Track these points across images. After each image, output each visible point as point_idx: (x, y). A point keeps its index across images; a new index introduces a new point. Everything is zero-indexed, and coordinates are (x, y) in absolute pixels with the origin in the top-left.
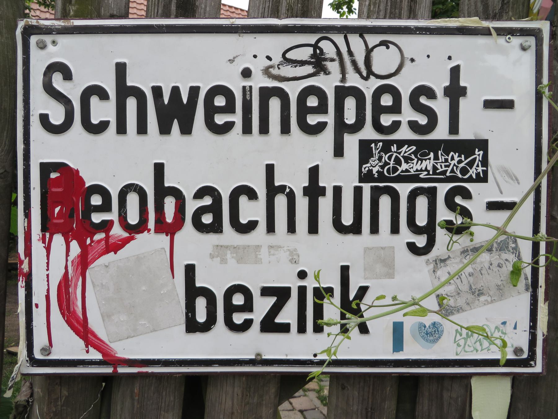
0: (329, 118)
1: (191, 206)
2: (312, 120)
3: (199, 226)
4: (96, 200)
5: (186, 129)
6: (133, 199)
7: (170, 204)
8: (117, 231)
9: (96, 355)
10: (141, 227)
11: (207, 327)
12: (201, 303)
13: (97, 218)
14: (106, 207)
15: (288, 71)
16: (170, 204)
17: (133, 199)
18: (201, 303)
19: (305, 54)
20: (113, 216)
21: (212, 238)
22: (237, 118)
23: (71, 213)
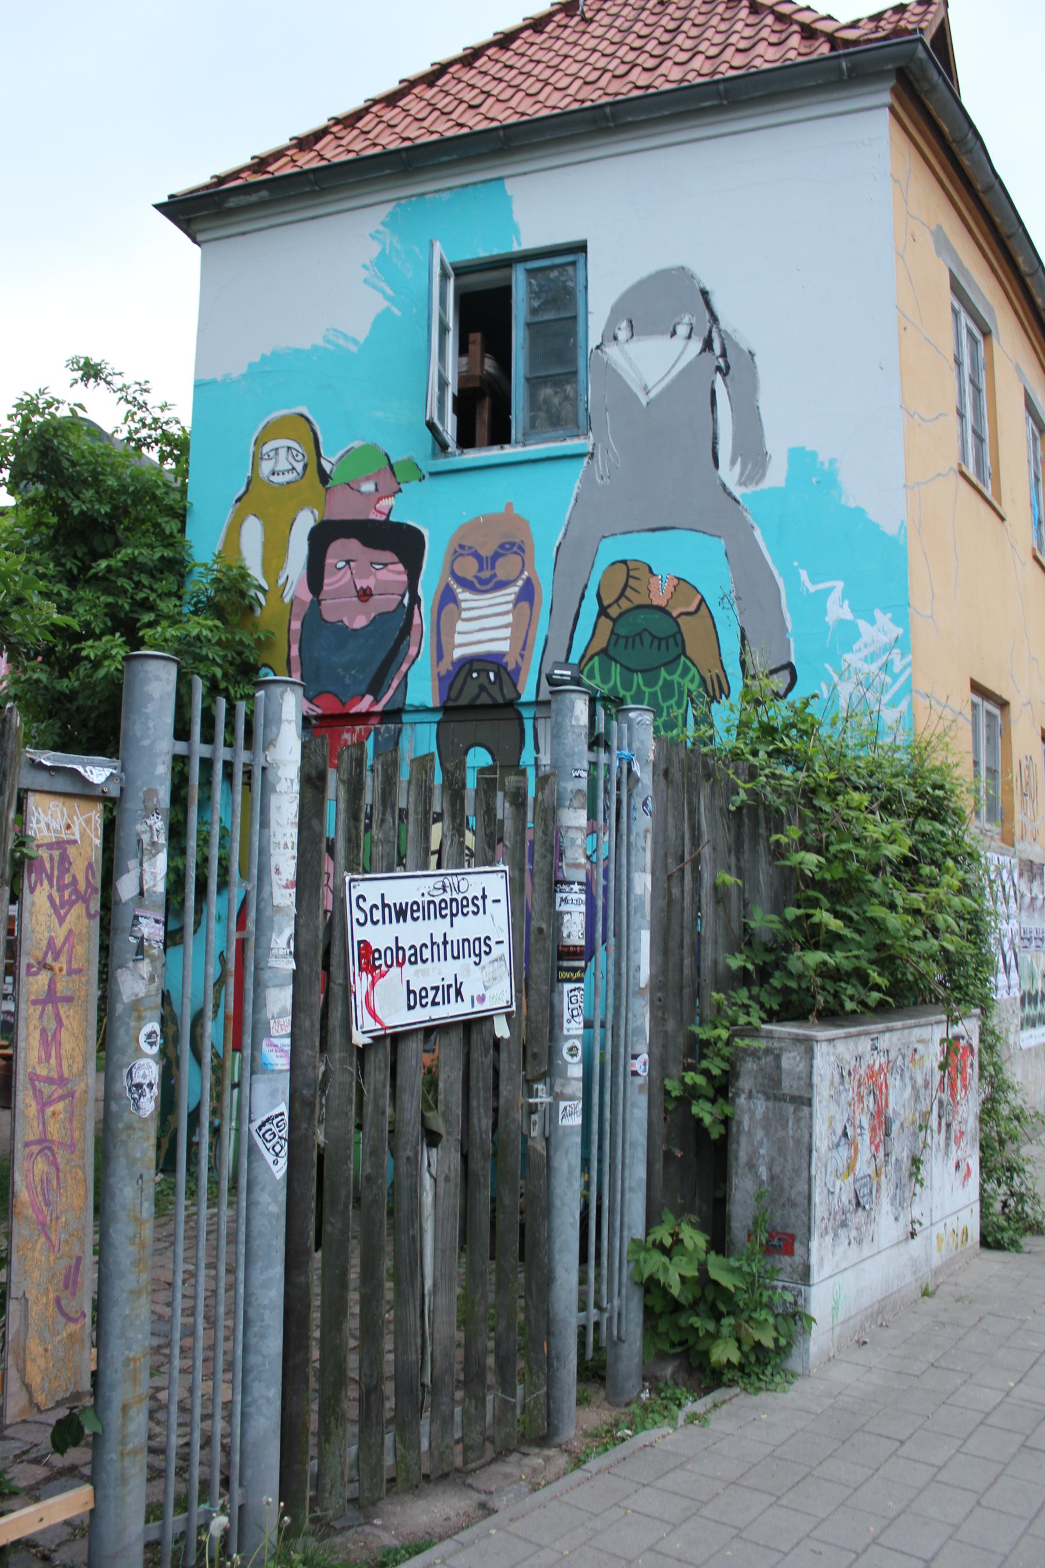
0: (448, 911)
1: (408, 953)
2: (444, 912)
3: (411, 963)
4: (377, 955)
5: (405, 920)
6: (389, 953)
7: (401, 953)
8: (384, 968)
9: (379, 1026)
10: (392, 965)
11: (413, 1008)
12: (412, 996)
13: (377, 963)
14: (380, 958)
15: (435, 893)
16: (401, 953)
17: (389, 953)
18: (412, 996)
19: (440, 885)
20: (382, 962)
21: (414, 967)
22: (420, 914)
23: (368, 963)
